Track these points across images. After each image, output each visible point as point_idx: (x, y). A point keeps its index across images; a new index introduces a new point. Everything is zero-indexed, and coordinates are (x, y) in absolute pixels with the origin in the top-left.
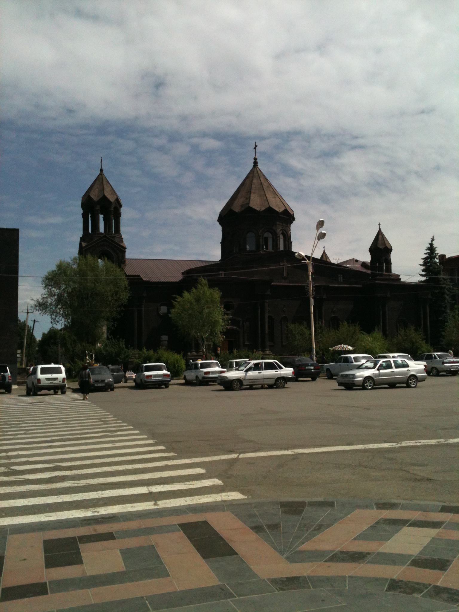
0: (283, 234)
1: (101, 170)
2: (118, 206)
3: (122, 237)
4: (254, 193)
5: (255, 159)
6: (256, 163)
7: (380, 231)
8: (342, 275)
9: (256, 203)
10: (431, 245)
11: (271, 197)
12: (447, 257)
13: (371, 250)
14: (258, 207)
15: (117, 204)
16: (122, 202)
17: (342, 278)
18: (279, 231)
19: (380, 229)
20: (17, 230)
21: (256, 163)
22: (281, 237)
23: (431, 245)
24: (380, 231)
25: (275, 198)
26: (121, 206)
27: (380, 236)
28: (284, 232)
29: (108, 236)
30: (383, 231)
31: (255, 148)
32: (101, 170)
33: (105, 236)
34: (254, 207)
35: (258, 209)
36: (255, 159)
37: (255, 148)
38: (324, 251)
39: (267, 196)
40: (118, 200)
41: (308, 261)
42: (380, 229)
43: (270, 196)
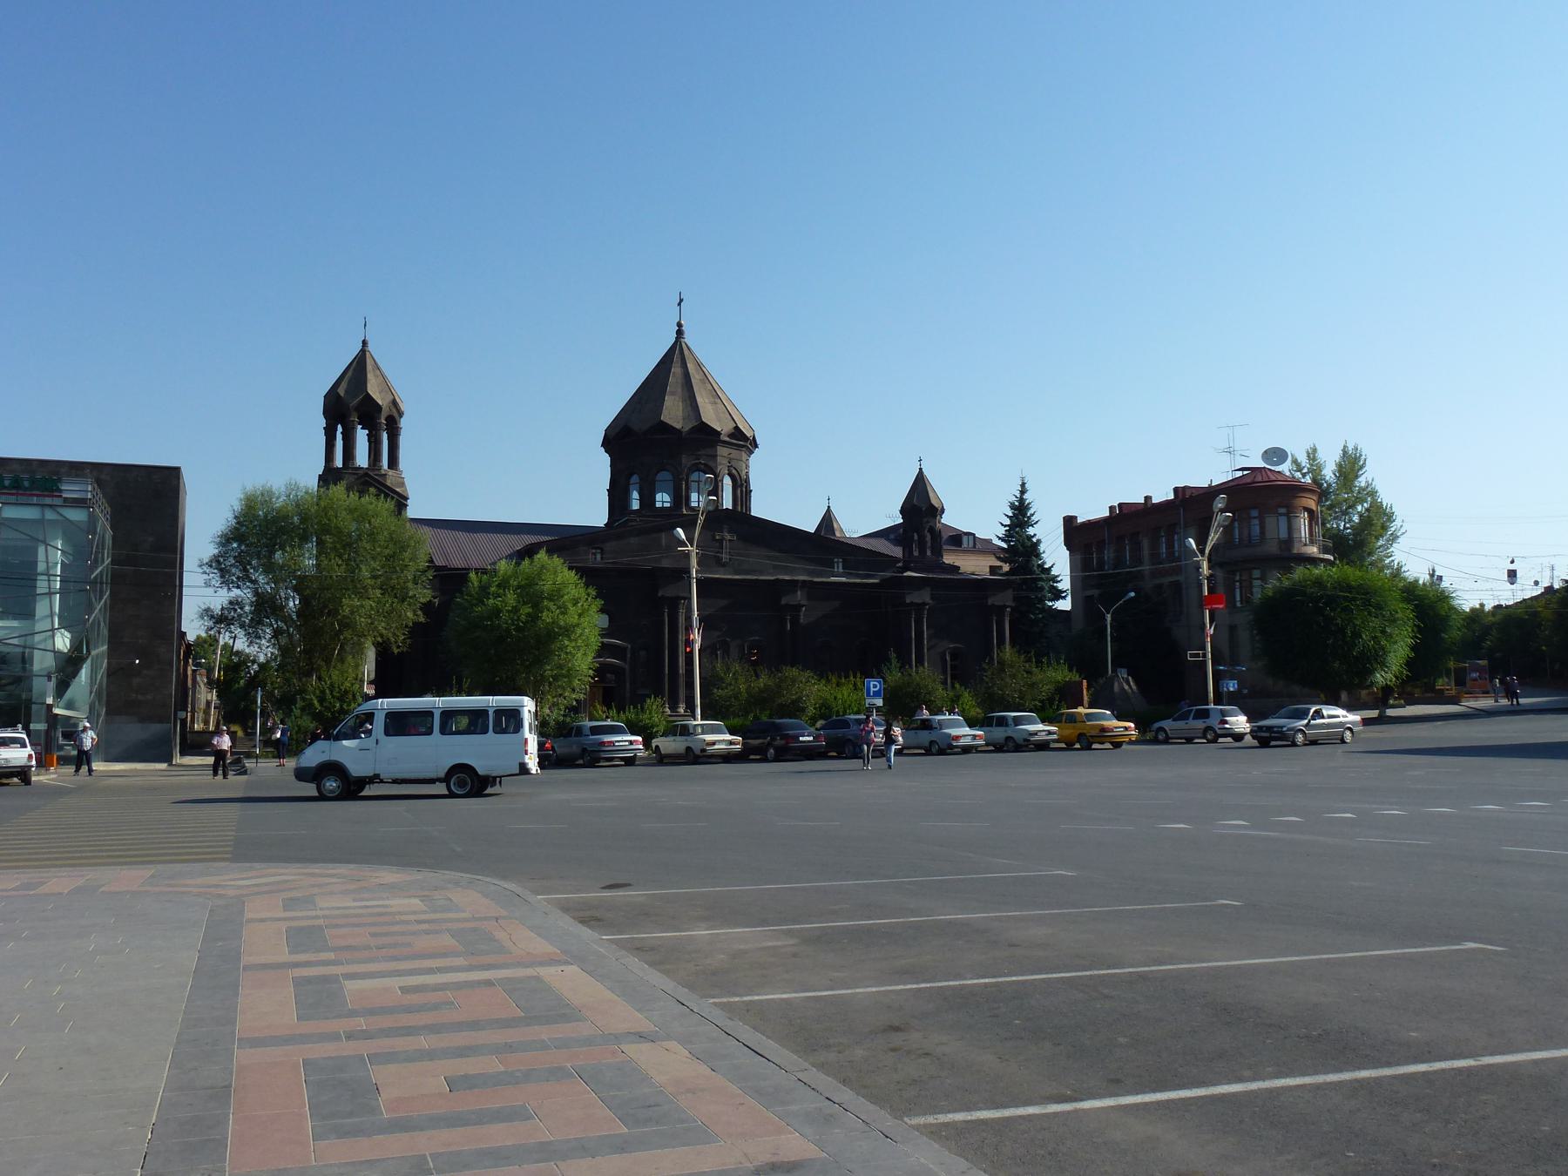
0: (730, 475)
1: (364, 343)
2: (396, 415)
3: (403, 476)
4: (673, 393)
5: (679, 325)
6: (680, 333)
7: (921, 474)
8: (841, 560)
9: (673, 412)
10: (1021, 500)
11: (707, 401)
12: (1080, 520)
13: (903, 511)
14: (678, 422)
15: (394, 410)
16: (403, 407)
17: (841, 565)
18: (722, 468)
19: (921, 469)
20: (175, 472)
21: (680, 333)
22: (727, 481)
23: (1021, 500)
24: (921, 474)
25: (716, 403)
26: (401, 414)
27: (920, 485)
28: (734, 471)
29: (371, 474)
30: (925, 472)
31: (679, 304)
32: (364, 343)
33: (366, 474)
34: (670, 422)
35: (678, 426)
36: (679, 325)
37: (679, 304)
38: (829, 507)
39: (699, 399)
40: (394, 403)
41: (690, 548)
42: (921, 469)
43: (702, 400)
